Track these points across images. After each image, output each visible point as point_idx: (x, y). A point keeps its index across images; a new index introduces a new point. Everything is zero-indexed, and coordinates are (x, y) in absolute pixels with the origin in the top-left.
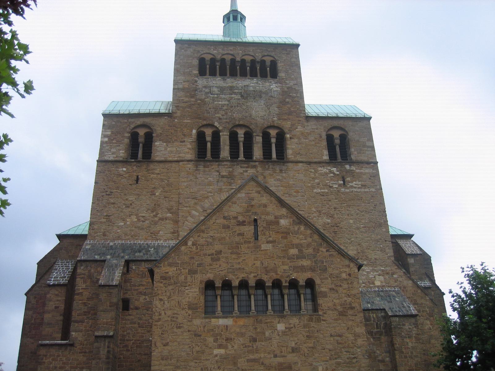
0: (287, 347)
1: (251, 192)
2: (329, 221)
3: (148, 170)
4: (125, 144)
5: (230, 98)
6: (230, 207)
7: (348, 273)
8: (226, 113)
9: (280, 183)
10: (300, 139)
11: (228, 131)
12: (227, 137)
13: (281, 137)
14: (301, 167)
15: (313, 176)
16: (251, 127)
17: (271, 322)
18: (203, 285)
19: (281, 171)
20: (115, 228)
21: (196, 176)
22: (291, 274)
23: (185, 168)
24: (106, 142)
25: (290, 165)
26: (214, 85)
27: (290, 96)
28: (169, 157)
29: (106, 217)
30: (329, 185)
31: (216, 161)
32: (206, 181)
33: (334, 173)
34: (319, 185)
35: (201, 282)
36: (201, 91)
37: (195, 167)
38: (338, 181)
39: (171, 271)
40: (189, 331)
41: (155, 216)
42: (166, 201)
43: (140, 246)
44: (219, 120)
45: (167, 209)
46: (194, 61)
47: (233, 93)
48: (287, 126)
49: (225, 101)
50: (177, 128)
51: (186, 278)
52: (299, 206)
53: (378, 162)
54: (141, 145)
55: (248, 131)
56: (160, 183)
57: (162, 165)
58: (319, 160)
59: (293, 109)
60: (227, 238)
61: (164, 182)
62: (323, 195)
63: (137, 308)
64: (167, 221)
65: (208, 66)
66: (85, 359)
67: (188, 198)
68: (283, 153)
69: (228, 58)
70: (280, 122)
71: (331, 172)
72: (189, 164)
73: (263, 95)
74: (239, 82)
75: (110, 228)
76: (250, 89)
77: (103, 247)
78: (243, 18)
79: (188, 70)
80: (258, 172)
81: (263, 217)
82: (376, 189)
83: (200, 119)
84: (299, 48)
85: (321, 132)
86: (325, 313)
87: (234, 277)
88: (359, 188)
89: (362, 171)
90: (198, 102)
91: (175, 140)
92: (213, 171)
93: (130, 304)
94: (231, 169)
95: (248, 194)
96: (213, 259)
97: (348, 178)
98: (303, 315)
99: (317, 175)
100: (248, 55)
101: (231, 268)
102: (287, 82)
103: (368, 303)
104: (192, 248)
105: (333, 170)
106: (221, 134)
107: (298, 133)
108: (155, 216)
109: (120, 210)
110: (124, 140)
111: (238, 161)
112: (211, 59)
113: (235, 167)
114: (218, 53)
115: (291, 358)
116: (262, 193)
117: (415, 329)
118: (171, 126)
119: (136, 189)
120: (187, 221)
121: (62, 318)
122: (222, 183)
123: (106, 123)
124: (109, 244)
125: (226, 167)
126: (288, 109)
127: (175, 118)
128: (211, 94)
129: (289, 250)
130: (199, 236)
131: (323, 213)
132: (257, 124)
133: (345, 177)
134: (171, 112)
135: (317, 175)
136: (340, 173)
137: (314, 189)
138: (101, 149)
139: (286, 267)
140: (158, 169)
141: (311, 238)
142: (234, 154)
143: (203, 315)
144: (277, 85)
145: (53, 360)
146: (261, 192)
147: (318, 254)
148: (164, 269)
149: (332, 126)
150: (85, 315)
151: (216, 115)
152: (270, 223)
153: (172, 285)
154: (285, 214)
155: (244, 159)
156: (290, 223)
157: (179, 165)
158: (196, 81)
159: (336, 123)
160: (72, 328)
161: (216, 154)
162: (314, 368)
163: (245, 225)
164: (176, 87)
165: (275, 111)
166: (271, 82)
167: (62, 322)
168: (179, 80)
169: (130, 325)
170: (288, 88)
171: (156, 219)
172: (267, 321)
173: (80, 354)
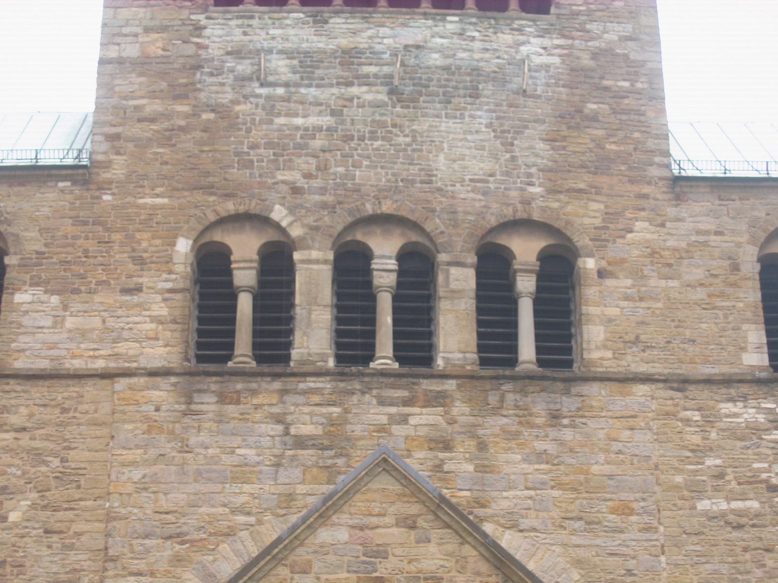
1: (374, 520)
5: (341, 102)
8: (323, 168)
9: (550, 471)
10: (643, 277)
11: (329, 243)
14: (642, 400)
15: (696, 439)
16: (428, 227)
19: (555, 417)
21: (182, 442)
23: (138, 403)
25: (596, 392)
26: (274, 44)
27: (606, 89)
28: (74, 357)
30: (766, 481)
31: (276, 376)
32: (227, 459)
34: (720, 482)
36: (218, 72)
37: (183, 400)
42: (49, 547)
44: (289, 198)
47: (357, 77)
48: (587, 221)
49: (320, 113)
50: (107, 230)
55: (416, 243)
56: (28, 468)
57: (38, 392)
58: (725, 369)
59: (613, 147)
61: (46, 463)
62: (739, 527)
67: (147, 536)
68: (569, 337)
70: (555, 205)
72: (156, 388)
73: (487, 89)
74: (383, 31)
76: (431, 63)
80: (455, 422)
83: (212, 194)
85: (739, 245)
90: (205, 116)
91: (98, 283)
92: (258, 416)
94: (336, 410)
95: (362, 529)
99: (713, 435)
106: (297, 256)
107: (636, 252)
111: (368, 375)
113: (355, 399)
116: (425, 525)
118: (85, 223)
122: (297, 473)
125: (316, 399)
126: (591, 146)
127: (102, 187)
132: (455, 212)
134: (85, 162)
135: (713, 435)
140: (23, 410)
144: (547, 42)
146: (421, 522)
155: (396, 365)
157: (114, 392)
158: (198, 29)
164: (113, 53)
165: (537, 156)
166: (520, 30)
168: (127, 25)
170: (595, 56)
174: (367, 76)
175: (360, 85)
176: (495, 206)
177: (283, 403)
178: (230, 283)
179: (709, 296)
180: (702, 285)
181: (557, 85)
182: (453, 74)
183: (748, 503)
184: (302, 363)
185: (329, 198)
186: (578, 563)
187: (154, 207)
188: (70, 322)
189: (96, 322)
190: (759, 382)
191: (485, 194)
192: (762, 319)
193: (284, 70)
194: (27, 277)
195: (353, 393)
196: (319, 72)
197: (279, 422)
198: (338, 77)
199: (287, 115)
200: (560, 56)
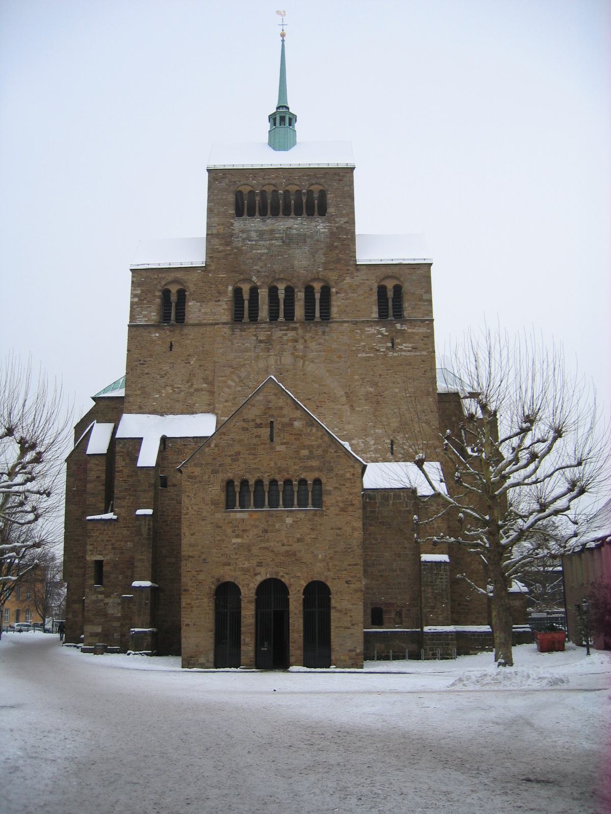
3: (182, 335)
4: (156, 306)
7: (352, 473)
8: (265, 265)
13: (326, 292)
15: (359, 338)
17: (282, 516)
18: (224, 484)
19: (324, 333)
22: (301, 474)
25: (334, 325)
27: (340, 238)
30: (375, 348)
33: (382, 334)
38: (386, 343)
39: (197, 471)
45: (203, 379)
51: (209, 477)
52: (341, 374)
53: (433, 320)
54: (173, 304)
59: (340, 256)
64: (204, 392)
71: (380, 333)
72: (223, 328)
73: (308, 240)
76: (294, 233)
78: (292, 119)
79: (223, 210)
81: (279, 419)
82: (428, 352)
85: (372, 283)
86: (328, 509)
87: (250, 476)
88: (409, 351)
89: (414, 331)
90: (234, 251)
92: (250, 334)
94: (269, 333)
96: (233, 460)
97: (397, 339)
99: (363, 337)
100: (293, 184)
102: (337, 219)
104: (214, 450)
112: (250, 192)
113: (274, 330)
115: (297, 547)
120: (223, 392)
121: (103, 488)
123: (135, 279)
125: (264, 330)
127: (210, 272)
128: (249, 241)
130: (220, 439)
137: (359, 353)
138: (131, 312)
141: (321, 439)
142: (274, 316)
143: (224, 510)
144: (324, 225)
145: (100, 534)
146: (279, 395)
147: (327, 455)
150: (127, 492)
152: (284, 425)
153: (197, 483)
158: (232, 224)
159: (389, 272)
161: (254, 317)
163: (262, 427)
166: (317, 221)
167: (104, 492)
168: (213, 223)
169: (169, 502)
170: (337, 228)
171: (192, 390)
172: (277, 515)
174: (277, 237)
176: (309, 275)
177: (256, 331)
178: (242, 297)
179: (364, 298)
181: (327, 238)
185: (267, 274)
186: (328, 371)
188: (203, 311)
189: (209, 310)
190: (375, 322)
191: (307, 271)
195: (272, 328)
196: (264, 237)
197: (255, 336)
198: (269, 238)
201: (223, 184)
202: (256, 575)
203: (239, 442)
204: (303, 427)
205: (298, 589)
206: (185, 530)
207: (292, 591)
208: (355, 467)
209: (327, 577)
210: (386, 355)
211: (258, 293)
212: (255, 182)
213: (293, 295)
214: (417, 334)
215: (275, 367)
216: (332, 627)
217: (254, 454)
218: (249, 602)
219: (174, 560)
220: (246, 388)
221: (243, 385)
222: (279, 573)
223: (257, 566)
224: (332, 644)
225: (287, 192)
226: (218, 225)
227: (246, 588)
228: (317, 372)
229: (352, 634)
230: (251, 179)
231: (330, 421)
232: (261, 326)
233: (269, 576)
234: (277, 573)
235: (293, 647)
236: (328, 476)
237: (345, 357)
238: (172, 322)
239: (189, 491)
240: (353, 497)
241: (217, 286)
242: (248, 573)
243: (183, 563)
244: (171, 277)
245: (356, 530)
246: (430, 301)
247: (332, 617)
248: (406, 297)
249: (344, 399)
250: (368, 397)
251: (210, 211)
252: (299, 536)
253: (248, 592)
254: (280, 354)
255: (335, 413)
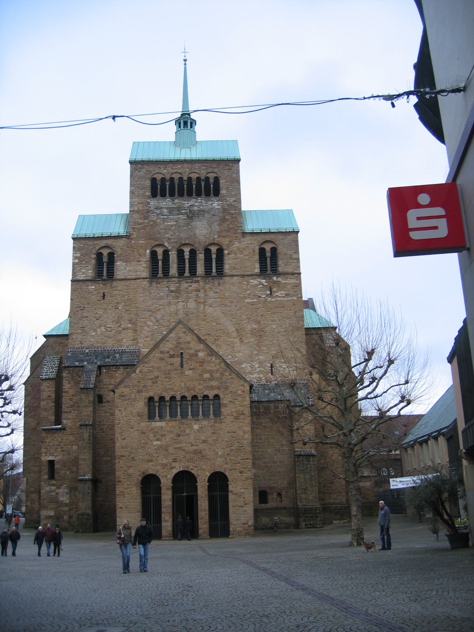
0: (200, 439)
2: (256, 326)
3: (112, 287)
6: (165, 344)
7: (242, 390)
8: (174, 234)
11: (176, 250)
12: (175, 256)
15: (245, 288)
18: (147, 400)
19: (219, 284)
20: (89, 337)
24: (77, 264)
25: (226, 279)
27: (230, 213)
28: (129, 276)
29: (81, 329)
30: (258, 295)
31: (167, 278)
33: (263, 285)
35: (145, 398)
38: (266, 291)
39: (126, 391)
40: (138, 430)
41: (119, 326)
43: (109, 353)
45: (129, 320)
46: (147, 181)
48: (226, 243)
49: (173, 222)
50: (133, 248)
51: (136, 396)
54: (105, 264)
57: (123, 283)
58: (251, 273)
59: (231, 226)
60: (162, 367)
62: (253, 305)
63: (108, 402)
65: (159, 186)
66: (74, 439)
69: (176, 177)
71: (261, 283)
75: (85, 337)
77: (81, 354)
78: (193, 123)
81: (187, 351)
82: (297, 298)
83: (153, 240)
84: (241, 163)
85: (255, 246)
86: (225, 418)
87: (166, 394)
88: (283, 297)
89: (286, 281)
93: (103, 399)
94: (178, 285)
95: (177, 334)
98: (210, 419)
99: (249, 287)
101: (164, 388)
103: (279, 394)
105: (262, 282)
106: (170, 253)
108: (119, 326)
109: (92, 322)
110: (91, 261)
114: (166, 172)
115: (202, 446)
117: (310, 415)
119: (103, 304)
120: (143, 330)
121: (53, 404)
123: (75, 245)
124: (85, 351)
125: (174, 283)
127: (132, 239)
128: (162, 216)
129: (204, 374)
130: (143, 366)
131: (252, 320)
132: (200, 242)
133: (272, 288)
136: (268, 284)
138: (73, 270)
139: (201, 387)
141: (219, 365)
142: (181, 272)
143: (147, 420)
144: (218, 203)
146: (186, 332)
148: (121, 389)
149: (265, 241)
150: (72, 408)
151: (166, 236)
152: (192, 355)
153: (127, 400)
154: (202, 348)
156: (205, 355)
159: (268, 237)
160: (63, 417)
162: (216, 453)
163: (175, 357)
164: (132, 209)
165: (216, 229)
167: (54, 408)
171: (120, 329)
173: (70, 435)
174: (182, 213)
175: (181, 215)
176: (208, 240)
177: (168, 283)
178: (157, 257)
179: (249, 257)
180: (248, 255)
182: (199, 211)
183: (255, 300)
184: (171, 275)
185: (176, 240)
186: (223, 313)
187: (142, 243)
191: (206, 238)
192: (259, 262)
193: (166, 212)
194: (119, 259)
195: (181, 281)
196: (173, 212)
197: (168, 287)
199: (167, 222)
200: (221, 206)
201: (142, 173)
202: (172, 468)
203: (157, 369)
204: (205, 357)
205: (203, 478)
206: (117, 435)
207: (199, 480)
208: (245, 386)
209: (225, 469)
210: (266, 300)
211: (169, 255)
212: (166, 171)
213: (195, 256)
214: (289, 284)
215: (183, 311)
216: (230, 506)
217: (169, 378)
218: (167, 489)
219: (109, 459)
220: (162, 326)
221: (159, 324)
222: (189, 466)
223: (173, 462)
224: (230, 519)
225: (190, 179)
226: (139, 203)
227: (165, 478)
228: (214, 314)
229: (245, 511)
230: (162, 169)
231: (225, 350)
232: (172, 280)
233: (182, 469)
234: (188, 467)
235: (201, 522)
236: (225, 393)
237: (236, 302)
238: (104, 278)
239: (121, 406)
240: (244, 408)
241: (138, 250)
242: (166, 467)
243: (117, 461)
244: (103, 243)
245: (246, 433)
246: (298, 260)
247: (230, 499)
248: (280, 257)
249: (235, 334)
250: (253, 332)
251: (132, 193)
252: (203, 438)
253: (166, 482)
254: (186, 301)
255: (228, 345)
